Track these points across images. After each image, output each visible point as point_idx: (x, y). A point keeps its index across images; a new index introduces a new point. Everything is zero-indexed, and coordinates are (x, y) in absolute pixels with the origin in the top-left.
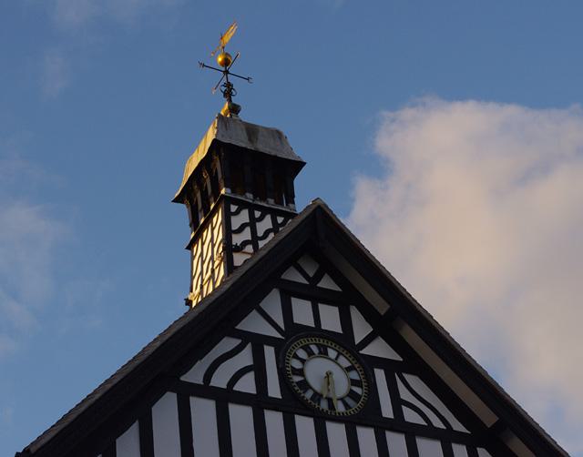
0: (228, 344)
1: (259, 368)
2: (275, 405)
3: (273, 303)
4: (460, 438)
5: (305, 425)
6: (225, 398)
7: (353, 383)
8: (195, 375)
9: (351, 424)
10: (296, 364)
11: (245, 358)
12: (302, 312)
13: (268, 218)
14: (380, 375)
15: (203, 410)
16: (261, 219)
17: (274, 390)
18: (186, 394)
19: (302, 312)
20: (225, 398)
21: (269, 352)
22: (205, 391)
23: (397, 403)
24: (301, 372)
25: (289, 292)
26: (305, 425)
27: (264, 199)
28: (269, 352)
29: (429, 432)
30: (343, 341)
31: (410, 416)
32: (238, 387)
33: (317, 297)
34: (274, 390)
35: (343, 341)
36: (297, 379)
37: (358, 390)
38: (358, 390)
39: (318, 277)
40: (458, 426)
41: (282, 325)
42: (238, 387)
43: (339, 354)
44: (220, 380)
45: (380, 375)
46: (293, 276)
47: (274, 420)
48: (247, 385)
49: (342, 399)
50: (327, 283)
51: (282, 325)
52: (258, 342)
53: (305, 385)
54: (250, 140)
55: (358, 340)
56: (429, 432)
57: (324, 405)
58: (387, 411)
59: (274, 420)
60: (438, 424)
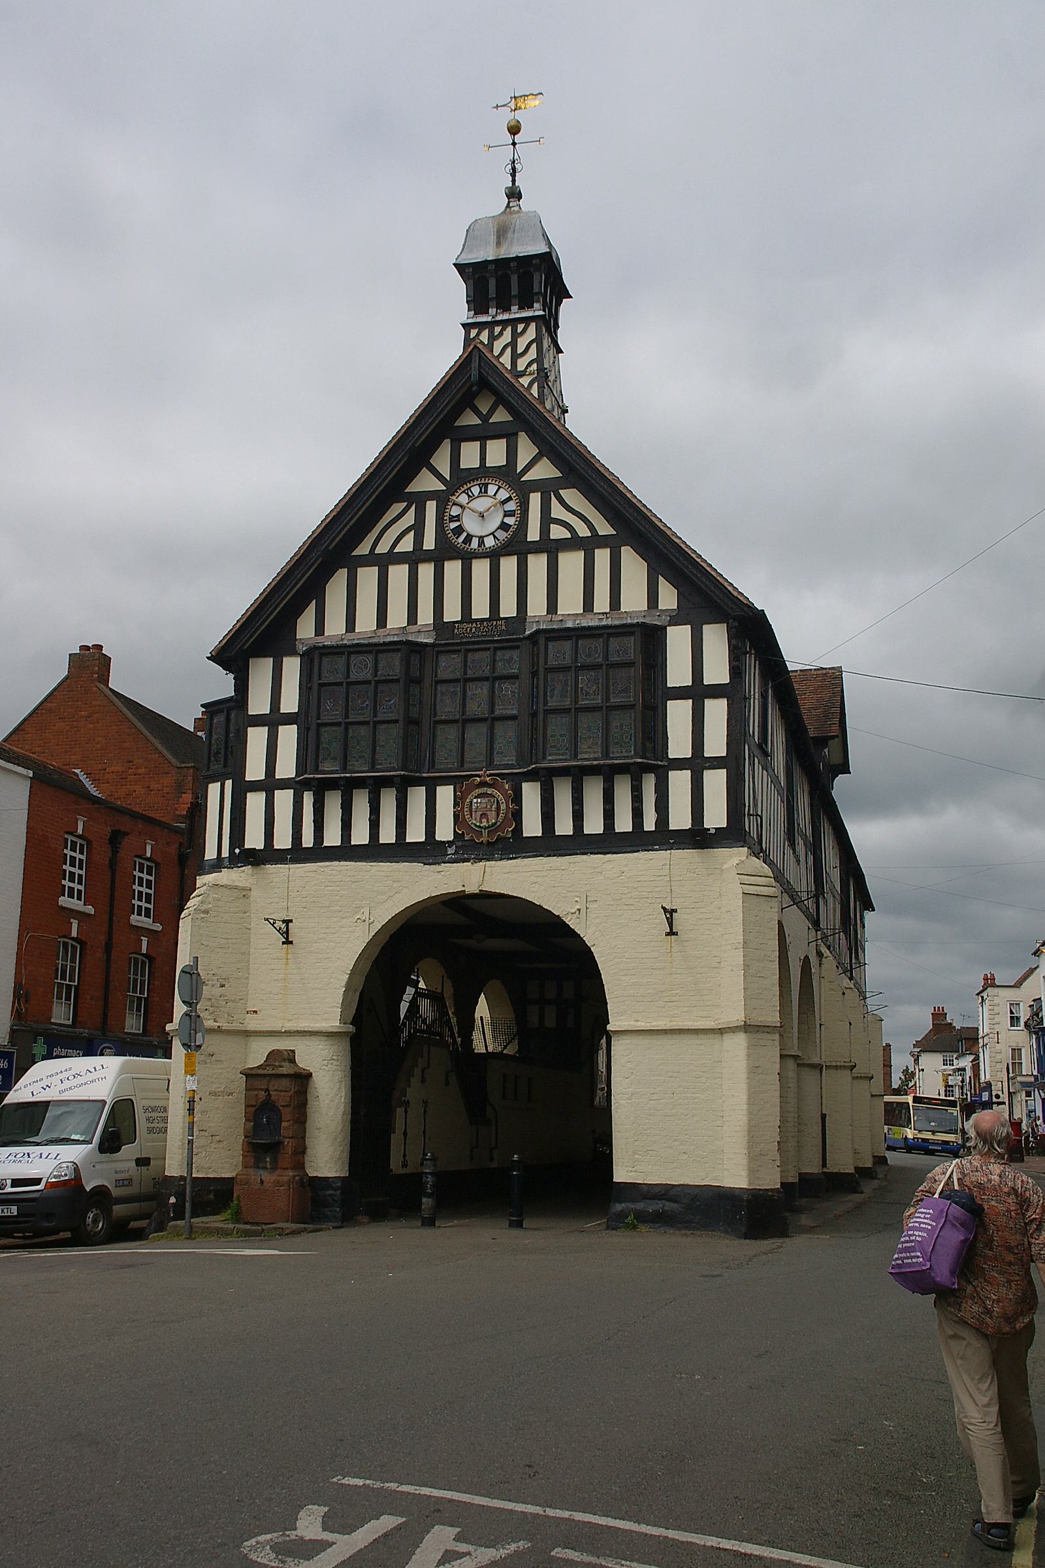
0: (398, 507)
1: (418, 528)
2: (427, 557)
5: (453, 569)
6: (383, 562)
7: (507, 514)
8: (363, 549)
9: (494, 556)
10: (455, 511)
11: (409, 519)
12: (470, 456)
14: (535, 499)
15: (368, 577)
16: (501, 334)
17: (429, 543)
18: (354, 565)
19: (470, 456)
21: (431, 507)
22: (372, 559)
23: (547, 520)
25: (460, 436)
26: (453, 569)
27: (507, 309)
28: (431, 507)
29: (574, 543)
31: (557, 532)
33: (482, 435)
35: (508, 474)
36: (453, 525)
37: (510, 521)
38: (510, 521)
39: (492, 411)
40: (604, 529)
44: (383, 548)
45: (535, 499)
46: (470, 419)
47: (426, 572)
48: (407, 545)
49: (493, 534)
50: (501, 416)
52: (419, 501)
53: (459, 530)
54: (498, 244)
56: (574, 543)
58: (533, 535)
59: (426, 572)
60: (583, 531)
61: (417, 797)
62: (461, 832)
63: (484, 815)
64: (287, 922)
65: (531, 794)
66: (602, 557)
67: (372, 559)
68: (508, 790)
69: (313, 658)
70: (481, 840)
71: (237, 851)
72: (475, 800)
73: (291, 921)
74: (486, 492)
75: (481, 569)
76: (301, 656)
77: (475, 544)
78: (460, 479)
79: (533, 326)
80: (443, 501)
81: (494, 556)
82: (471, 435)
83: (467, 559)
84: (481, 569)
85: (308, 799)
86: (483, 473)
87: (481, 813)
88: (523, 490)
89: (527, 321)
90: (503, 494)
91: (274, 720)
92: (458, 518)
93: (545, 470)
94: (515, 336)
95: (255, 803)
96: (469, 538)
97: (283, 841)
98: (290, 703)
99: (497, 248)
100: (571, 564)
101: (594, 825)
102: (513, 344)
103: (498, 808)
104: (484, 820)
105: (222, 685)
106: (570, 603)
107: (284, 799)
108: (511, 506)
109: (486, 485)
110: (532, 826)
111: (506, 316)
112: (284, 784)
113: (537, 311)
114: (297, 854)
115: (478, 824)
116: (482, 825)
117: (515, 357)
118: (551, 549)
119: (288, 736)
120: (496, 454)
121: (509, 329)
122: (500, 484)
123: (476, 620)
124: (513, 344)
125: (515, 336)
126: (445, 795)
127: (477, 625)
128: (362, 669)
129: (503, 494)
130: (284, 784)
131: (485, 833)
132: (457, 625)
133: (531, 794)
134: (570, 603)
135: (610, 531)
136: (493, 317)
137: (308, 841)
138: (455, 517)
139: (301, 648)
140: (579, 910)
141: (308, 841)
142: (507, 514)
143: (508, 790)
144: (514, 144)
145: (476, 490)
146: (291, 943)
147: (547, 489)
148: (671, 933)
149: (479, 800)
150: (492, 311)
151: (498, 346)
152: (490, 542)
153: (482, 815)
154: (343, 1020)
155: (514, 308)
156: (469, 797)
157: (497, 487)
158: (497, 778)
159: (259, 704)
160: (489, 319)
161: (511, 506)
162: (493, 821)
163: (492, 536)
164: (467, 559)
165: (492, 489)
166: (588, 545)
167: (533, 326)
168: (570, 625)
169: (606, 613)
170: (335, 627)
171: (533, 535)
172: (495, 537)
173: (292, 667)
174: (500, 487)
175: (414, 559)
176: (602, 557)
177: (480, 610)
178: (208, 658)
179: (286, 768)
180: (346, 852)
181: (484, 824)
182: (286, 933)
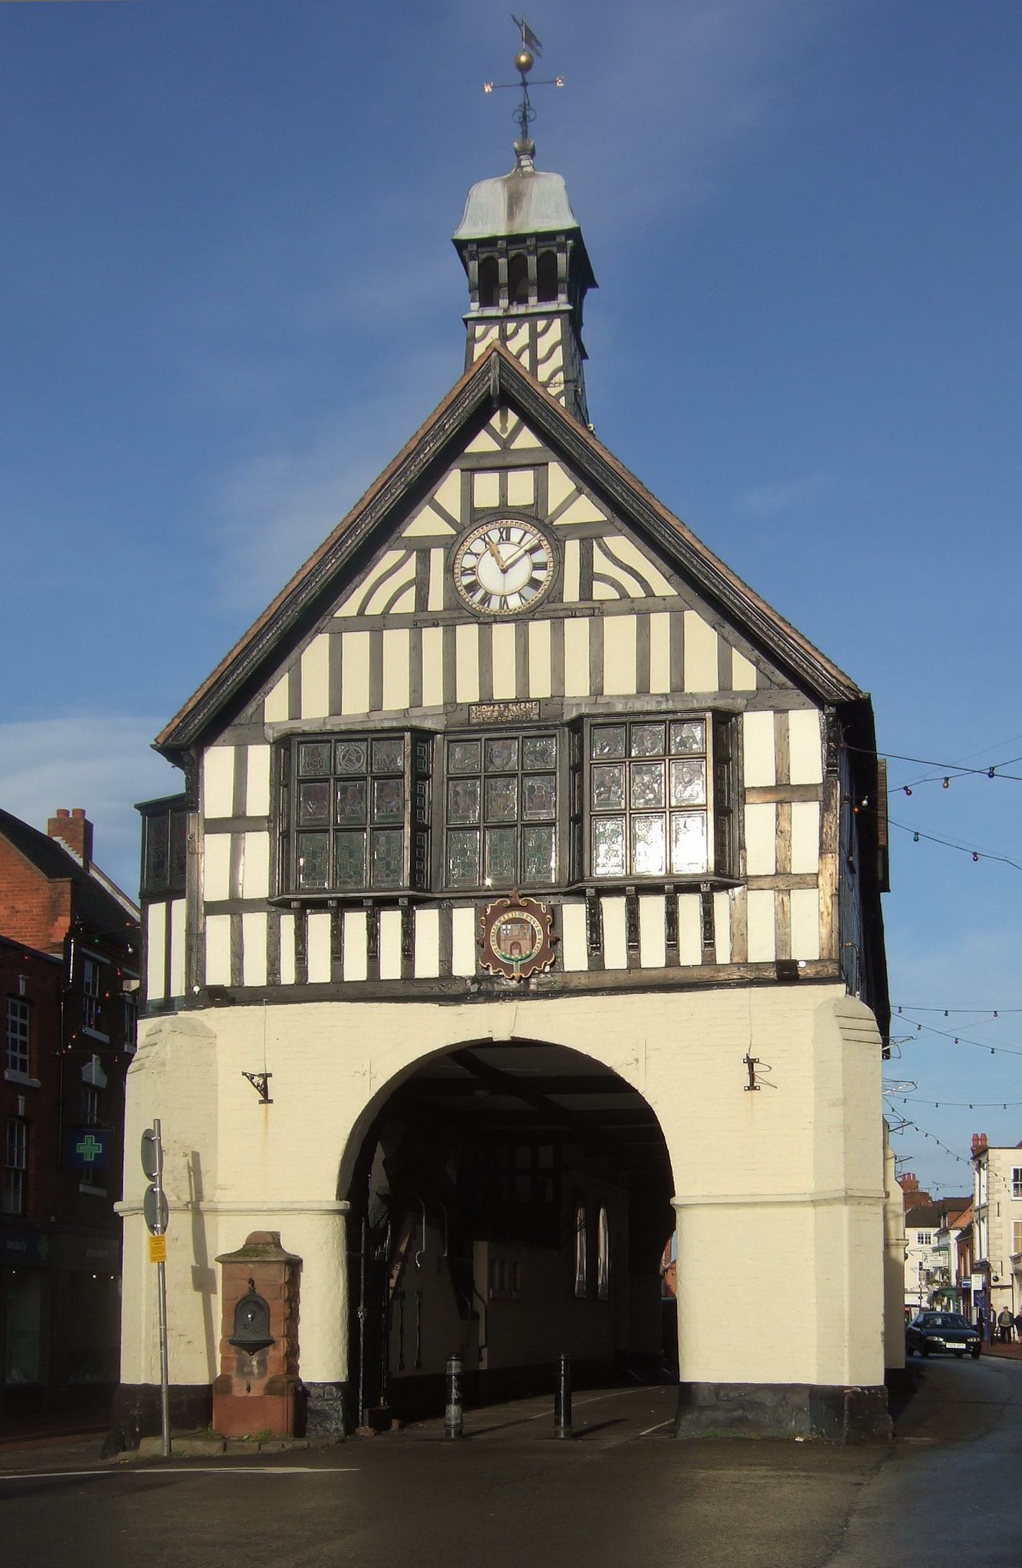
1: (421, 584)
3: (449, 491)
4: (663, 604)
6: (377, 626)
7: (536, 567)
8: (349, 608)
10: (468, 561)
11: (409, 571)
12: (487, 490)
13: (525, 329)
14: (573, 549)
15: (356, 645)
16: (515, 333)
17: (436, 602)
19: (487, 490)
20: (377, 626)
21: (437, 556)
22: (361, 621)
23: (588, 577)
24: (473, 571)
27: (523, 300)
28: (437, 556)
30: (535, 516)
31: (601, 591)
32: (396, 609)
33: (502, 465)
34: (436, 602)
35: (535, 516)
36: (467, 580)
40: (662, 587)
41: (456, 515)
42: (396, 609)
43: (526, 532)
44: (375, 608)
45: (573, 549)
49: (519, 592)
51: (456, 515)
52: (422, 549)
53: (473, 587)
54: (511, 215)
55: (552, 506)
56: (625, 604)
57: (495, 605)
58: (571, 593)
60: (635, 590)
61: (427, 920)
62: (485, 966)
63: (516, 945)
64: (266, 1076)
65: (574, 916)
66: (660, 623)
67: (361, 621)
68: (546, 914)
69: (284, 745)
70: (511, 976)
71: (196, 989)
72: (504, 927)
73: (270, 1075)
74: (508, 539)
75: (504, 635)
76: (271, 744)
77: (495, 605)
78: (476, 517)
79: (557, 323)
80: (451, 546)
81: (521, 619)
82: (484, 464)
83: (485, 622)
84: (504, 635)
85: (288, 923)
86: (503, 512)
87: (512, 942)
88: (554, 536)
89: (550, 316)
90: (530, 540)
91: (237, 824)
92: (473, 571)
93: (587, 511)
94: (534, 336)
95: (217, 929)
96: (486, 599)
97: (255, 976)
98: (259, 802)
99: (509, 220)
100: (621, 630)
101: (653, 955)
102: (532, 346)
103: (533, 938)
104: (516, 952)
105: (171, 781)
106: (620, 681)
107: (255, 925)
108: (541, 556)
109: (508, 530)
110: (575, 955)
111: (521, 310)
112: (254, 905)
113: (562, 302)
114: (273, 994)
115: (508, 956)
116: (513, 957)
117: (535, 362)
118: (595, 612)
119: (258, 846)
120: (521, 488)
121: (526, 327)
122: (527, 529)
123: (499, 702)
124: (532, 346)
125: (534, 336)
126: (464, 919)
127: (499, 707)
128: (348, 760)
129: (531, 540)
130: (254, 905)
131: (516, 966)
132: (474, 707)
133: (574, 916)
134: (620, 681)
135: (670, 591)
136: (505, 310)
137: (288, 975)
138: (469, 569)
139: (271, 734)
140: (637, 1060)
141: (288, 975)
142: (536, 567)
143: (546, 914)
144: (524, 84)
145: (495, 535)
146: (271, 1101)
147: (589, 536)
148: (752, 1087)
149: (509, 927)
150: (504, 303)
151: (514, 346)
152: (514, 603)
153: (513, 944)
154: (340, 1196)
155: (533, 300)
156: (496, 923)
157: (523, 532)
158: (532, 899)
159: (217, 802)
160: (500, 313)
161: (541, 556)
162: (528, 952)
163: (517, 594)
164: (485, 622)
165: (516, 535)
166: (642, 611)
167: (557, 323)
168: (619, 708)
169: (666, 695)
170: (315, 709)
171: (571, 593)
172: (521, 596)
173: (260, 758)
174: (526, 532)
175: (418, 621)
176: (660, 623)
177: (505, 688)
178: (152, 746)
179: (256, 882)
180: (338, 991)
181: (516, 955)
182: (264, 1090)
